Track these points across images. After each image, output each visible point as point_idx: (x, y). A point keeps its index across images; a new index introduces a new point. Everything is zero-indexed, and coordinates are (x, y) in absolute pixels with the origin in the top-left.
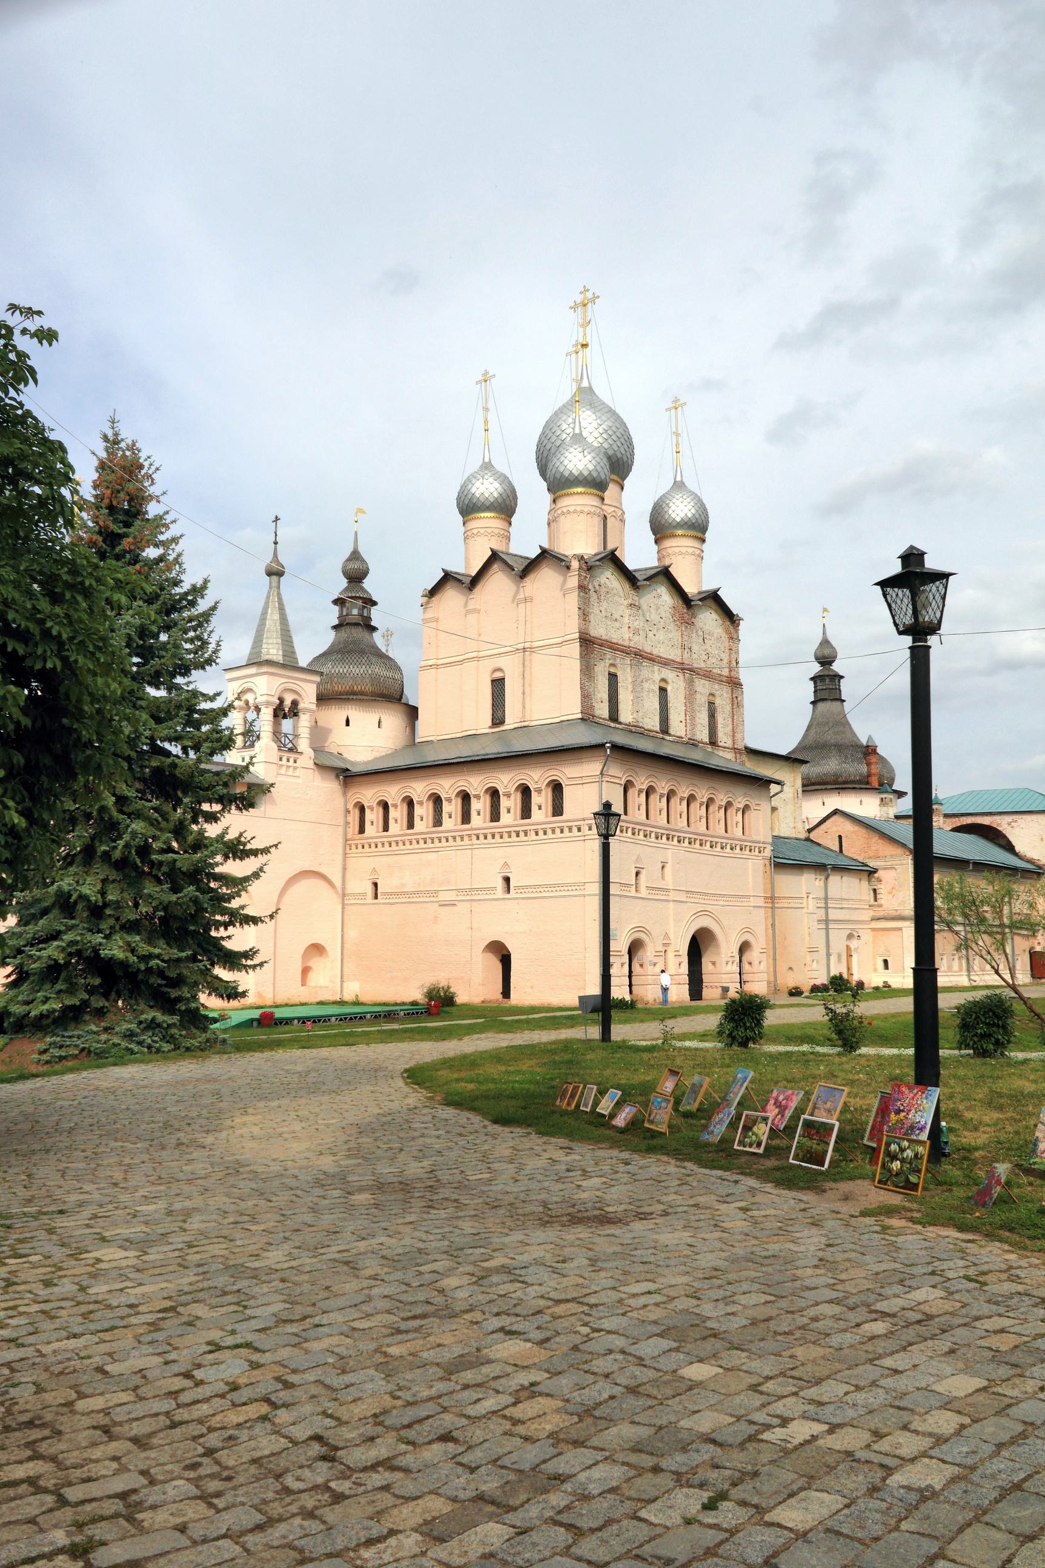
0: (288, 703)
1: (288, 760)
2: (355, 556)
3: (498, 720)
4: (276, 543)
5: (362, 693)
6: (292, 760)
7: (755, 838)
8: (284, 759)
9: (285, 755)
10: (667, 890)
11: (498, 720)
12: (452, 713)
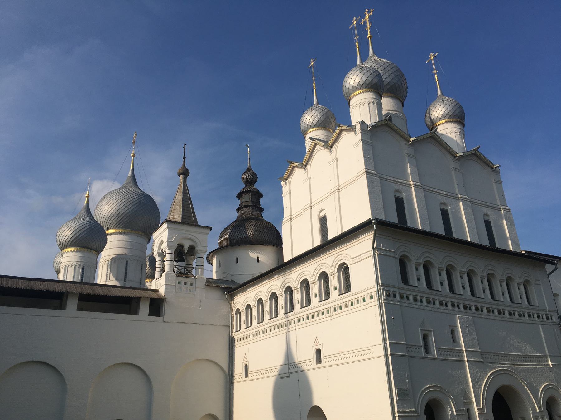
0: (186, 248)
1: (185, 283)
9: (183, 280)
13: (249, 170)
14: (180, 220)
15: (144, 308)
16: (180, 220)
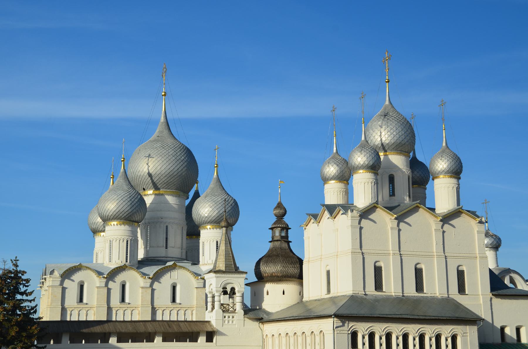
1: (229, 317)
2: (280, 206)
3: (329, 291)
5: (278, 277)
6: (231, 317)
9: (227, 315)
11: (329, 291)
12: (314, 288)
13: (280, 206)
14: (223, 268)
16: (223, 268)
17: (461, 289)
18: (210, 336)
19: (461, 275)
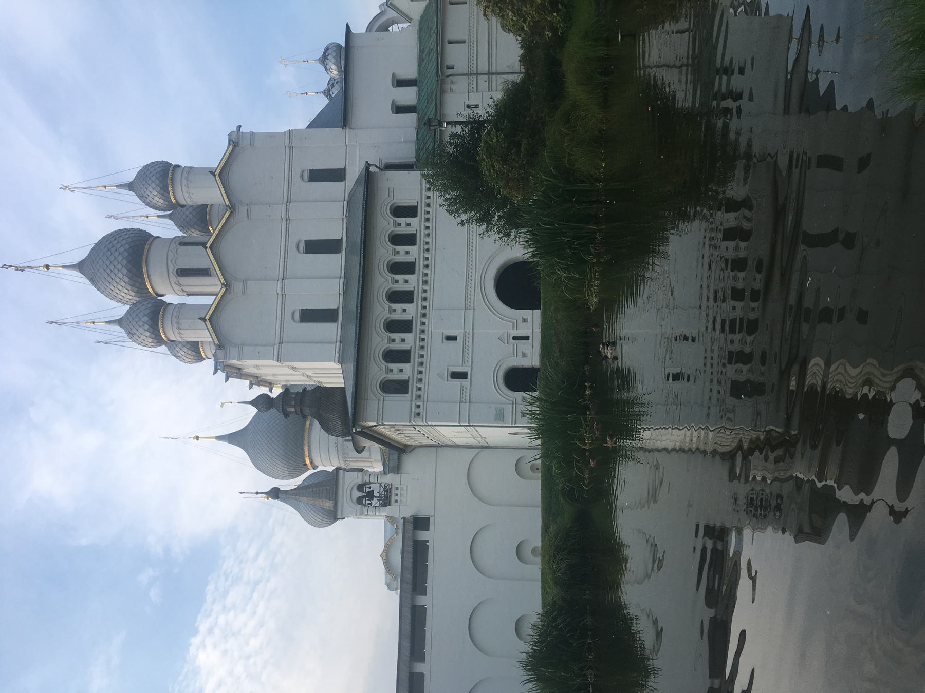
4: (257, 493)
6: (397, 492)
7: (418, 198)
8: (396, 498)
9: (393, 498)
10: (465, 332)
15: (423, 535)
17: (337, 175)
18: (421, 522)
19: (317, 176)
